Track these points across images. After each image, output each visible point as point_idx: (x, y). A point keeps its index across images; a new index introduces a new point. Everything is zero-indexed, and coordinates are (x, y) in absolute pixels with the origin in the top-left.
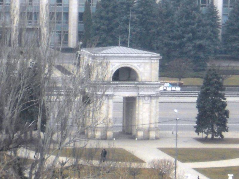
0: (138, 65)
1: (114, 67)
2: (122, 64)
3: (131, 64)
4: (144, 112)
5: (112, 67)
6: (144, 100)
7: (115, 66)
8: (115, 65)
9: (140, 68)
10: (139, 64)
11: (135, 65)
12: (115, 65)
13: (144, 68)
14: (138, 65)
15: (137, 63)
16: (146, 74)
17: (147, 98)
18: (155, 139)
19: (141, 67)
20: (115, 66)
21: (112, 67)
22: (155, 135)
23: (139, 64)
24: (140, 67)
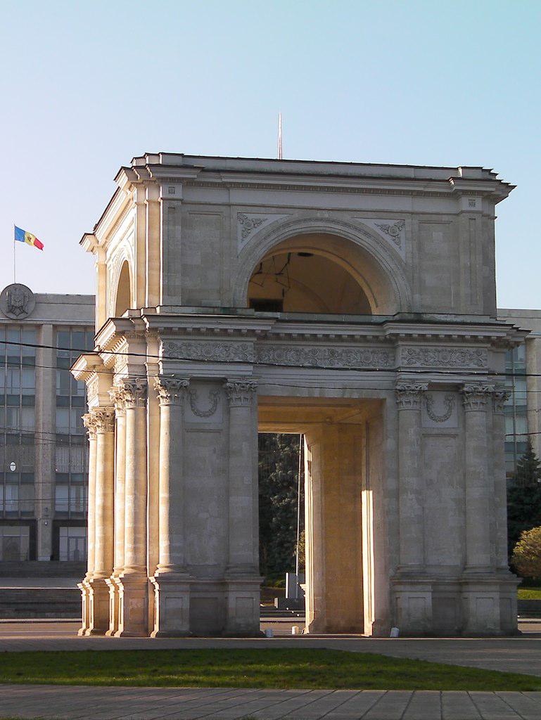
0: (385, 229)
1: (255, 231)
2: (297, 215)
3: (346, 217)
6: (425, 416)
7: (265, 224)
8: (260, 222)
10: (391, 223)
11: (371, 224)
12: (260, 222)
13: (420, 249)
14: (385, 229)
16: (430, 279)
17: (439, 404)
18: (498, 630)
19: (402, 234)
22: (497, 611)
23: (391, 223)
24: (396, 237)
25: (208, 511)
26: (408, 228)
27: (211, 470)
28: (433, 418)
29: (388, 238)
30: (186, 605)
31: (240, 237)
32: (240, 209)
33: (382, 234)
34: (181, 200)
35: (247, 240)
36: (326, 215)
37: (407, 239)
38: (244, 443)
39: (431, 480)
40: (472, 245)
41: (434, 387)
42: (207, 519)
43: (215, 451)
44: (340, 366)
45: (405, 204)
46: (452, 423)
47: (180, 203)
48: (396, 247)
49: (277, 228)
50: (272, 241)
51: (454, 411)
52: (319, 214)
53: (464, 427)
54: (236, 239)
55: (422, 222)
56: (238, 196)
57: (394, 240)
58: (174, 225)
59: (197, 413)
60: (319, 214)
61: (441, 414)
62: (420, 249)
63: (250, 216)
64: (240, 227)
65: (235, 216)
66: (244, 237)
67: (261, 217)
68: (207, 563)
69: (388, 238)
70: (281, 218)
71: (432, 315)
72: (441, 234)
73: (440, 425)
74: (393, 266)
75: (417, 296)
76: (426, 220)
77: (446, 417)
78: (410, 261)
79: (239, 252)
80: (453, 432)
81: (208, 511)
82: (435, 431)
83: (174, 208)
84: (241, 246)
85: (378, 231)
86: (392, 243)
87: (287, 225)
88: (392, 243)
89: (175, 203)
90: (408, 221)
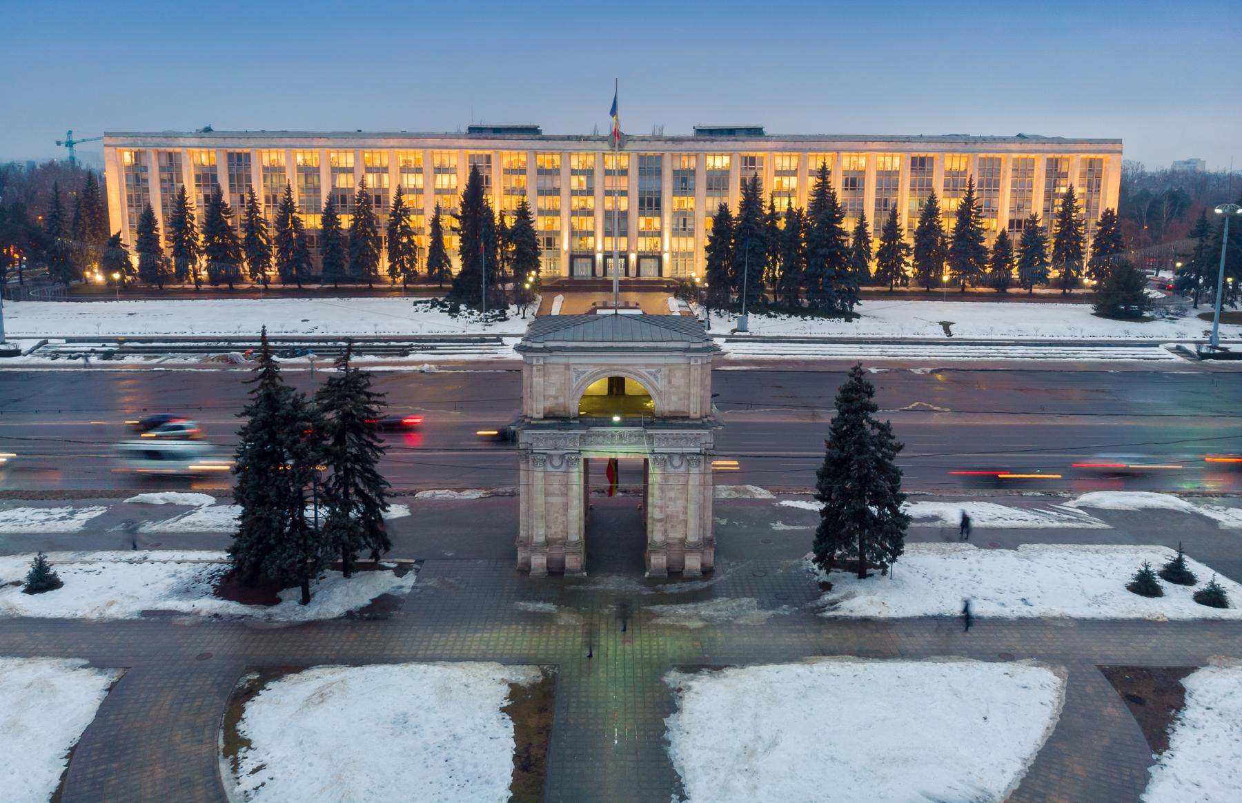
0: (651, 373)
1: (582, 377)
3: (630, 368)
5: (577, 377)
6: (669, 466)
7: (588, 373)
8: (584, 372)
10: (653, 370)
11: (643, 371)
12: (584, 372)
13: (670, 382)
14: (651, 373)
15: (647, 365)
18: (700, 574)
19: (659, 375)
21: (577, 377)
24: (656, 378)
26: (662, 372)
28: (674, 467)
29: (651, 378)
30: (545, 561)
32: (575, 367)
33: (649, 376)
36: (620, 367)
41: (670, 455)
46: (682, 469)
51: (684, 464)
52: (615, 367)
55: (670, 370)
56: (572, 361)
59: (553, 467)
60: (615, 367)
62: (670, 382)
64: (574, 375)
66: (576, 380)
70: (596, 370)
73: (676, 470)
76: (672, 369)
77: (680, 466)
84: (574, 385)
86: (653, 380)
90: (663, 369)
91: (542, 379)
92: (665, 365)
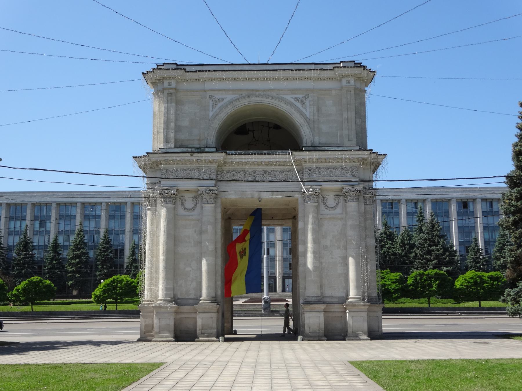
0: (297, 99)
3: (274, 94)
4: (326, 247)
5: (215, 104)
6: (322, 207)
7: (225, 101)
8: (223, 99)
9: (305, 108)
10: (300, 96)
11: (289, 97)
12: (223, 99)
13: (319, 110)
14: (297, 99)
15: (293, 91)
16: (324, 128)
19: (307, 103)
20: (225, 101)
24: (303, 103)
25: (191, 267)
27: (193, 242)
28: (327, 207)
29: (299, 105)
30: (172, 323)
31: (211, 109)
34: (175, 89)
35: (214, 110)
37: (310, 105)
38: (209, 226)
39: (326, 246)
40: (349, 106)
42: (190, 271)
43: (195, 232)
44: (270, 179)
45: (309, 85)
46: (339, 210)
47: (174, 91)
48: (304, 110)
49: (231, 102)
50: (230, 110)
51: (340, 204)
53: (346, 213)
54: (209, 110)
56: (208, 86)
57: (302, 106)
58: (171, 103)
61: (332, 206)
62: (319, 110)
63: (217, 97)
64: (211, 103)
65: (208, 96)
67: (223, 97)
68: (190, 297)
69: (299, 105)
71: (324, 147)
72: (332, 101)
73: (331, 212)
74: (302, 121)
75: (316, 138)
77: (335, 207)
78: (312, 118)
79: (210, 117)
80: (339, 216)
81: (191, 267)
82: (329, 216)
83: (171, 94)
84: (211, 114)
85: (293, 101)
87: (238, 99)
88: (301, 108)
89: (172, 91)
91: (173, 104)
92: (313, 90)
